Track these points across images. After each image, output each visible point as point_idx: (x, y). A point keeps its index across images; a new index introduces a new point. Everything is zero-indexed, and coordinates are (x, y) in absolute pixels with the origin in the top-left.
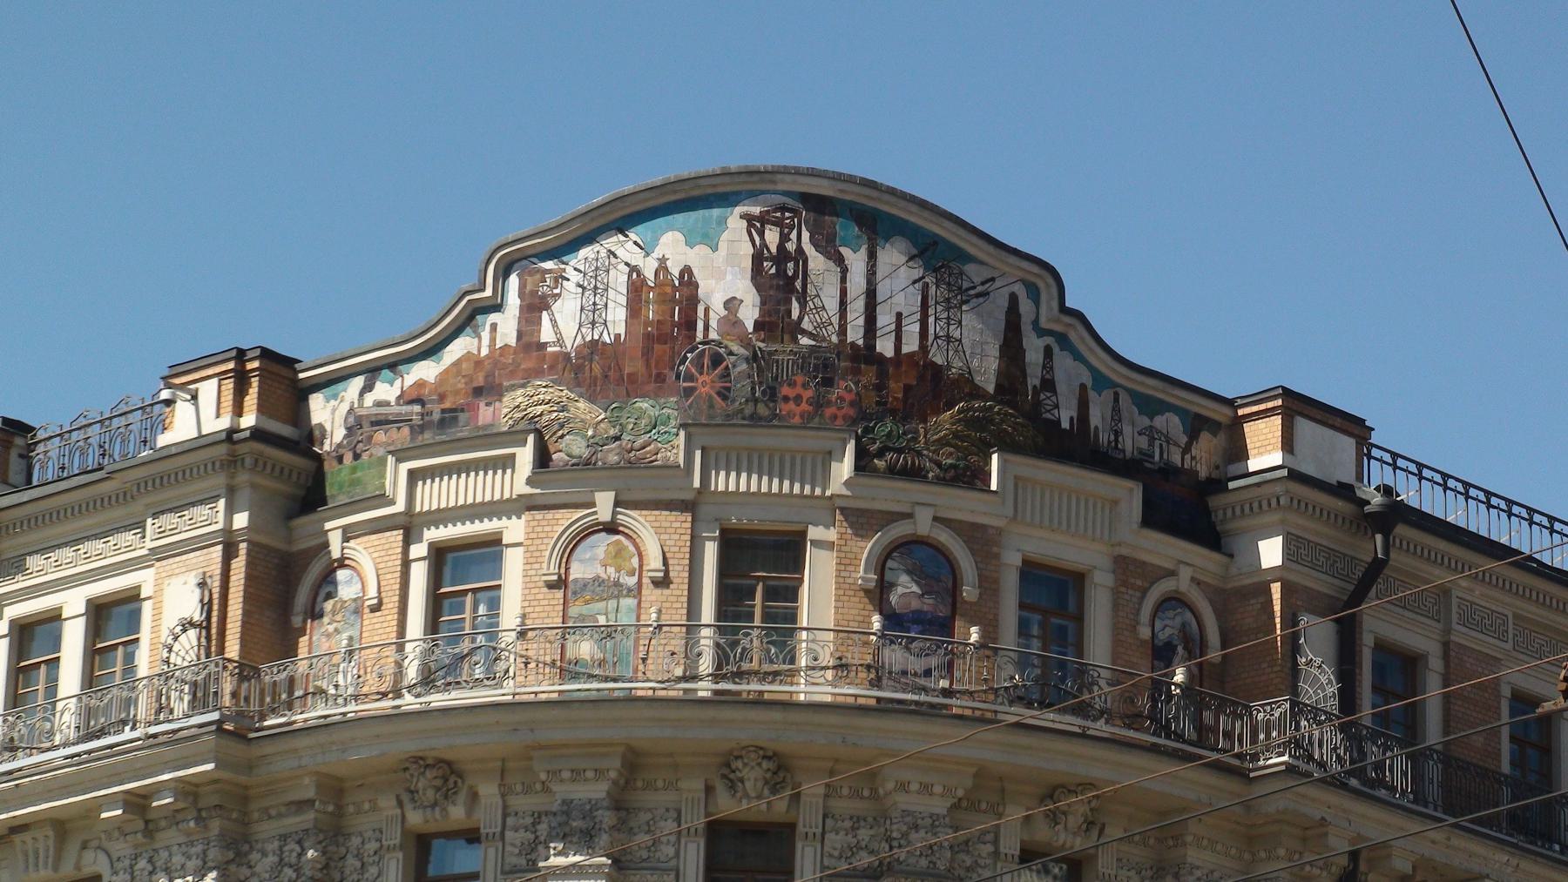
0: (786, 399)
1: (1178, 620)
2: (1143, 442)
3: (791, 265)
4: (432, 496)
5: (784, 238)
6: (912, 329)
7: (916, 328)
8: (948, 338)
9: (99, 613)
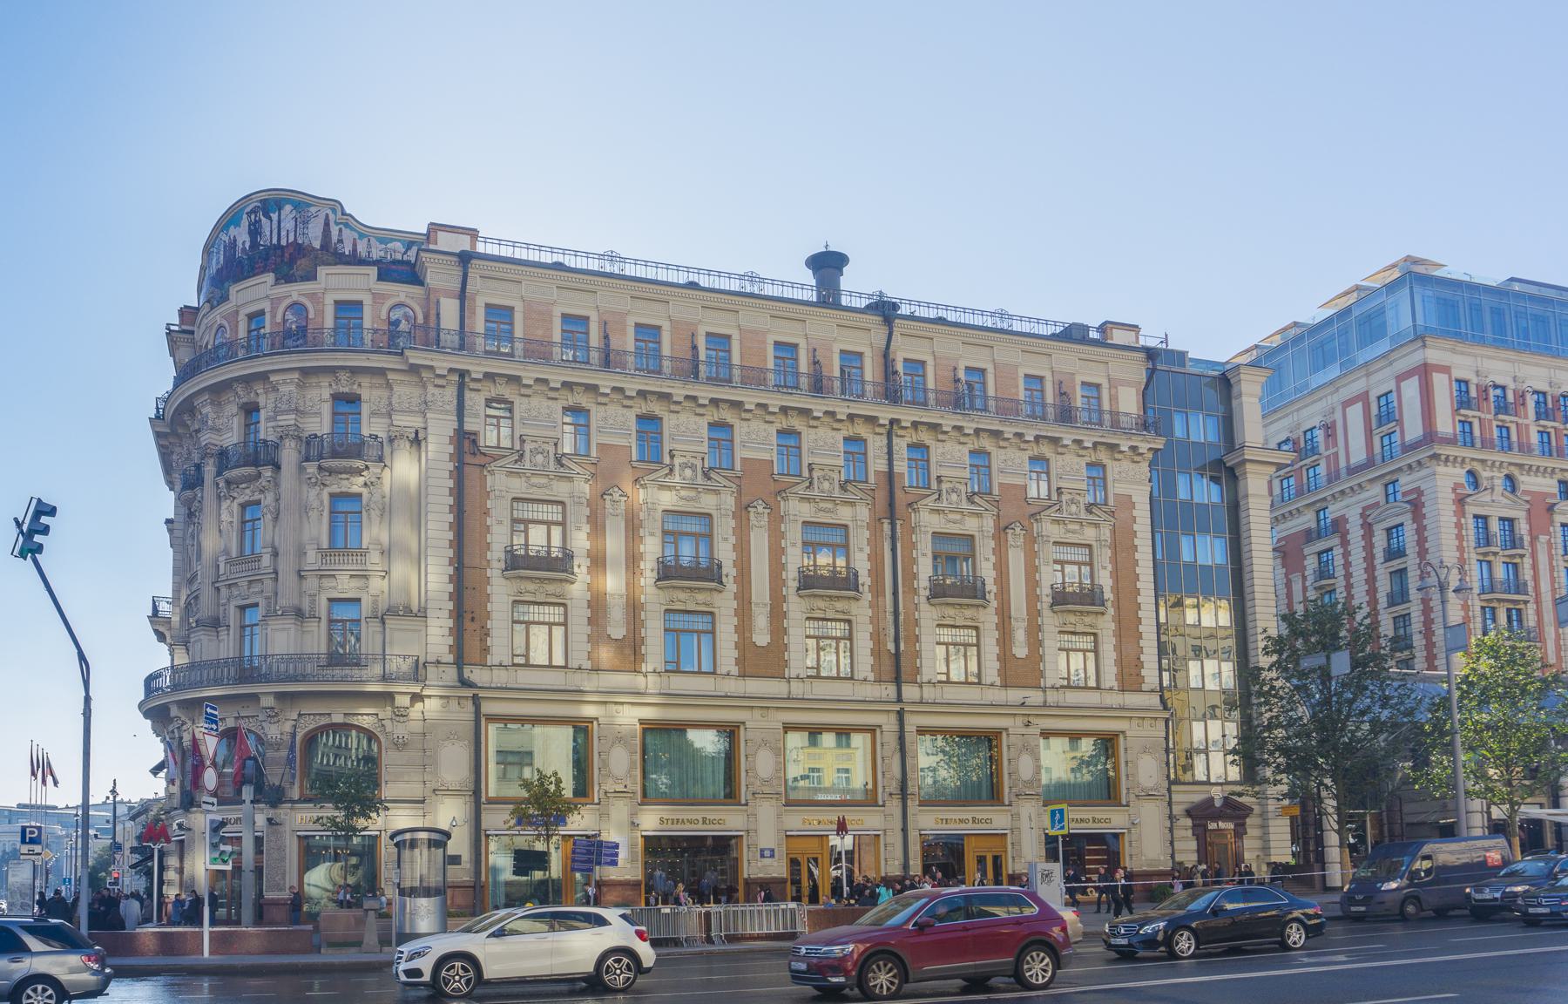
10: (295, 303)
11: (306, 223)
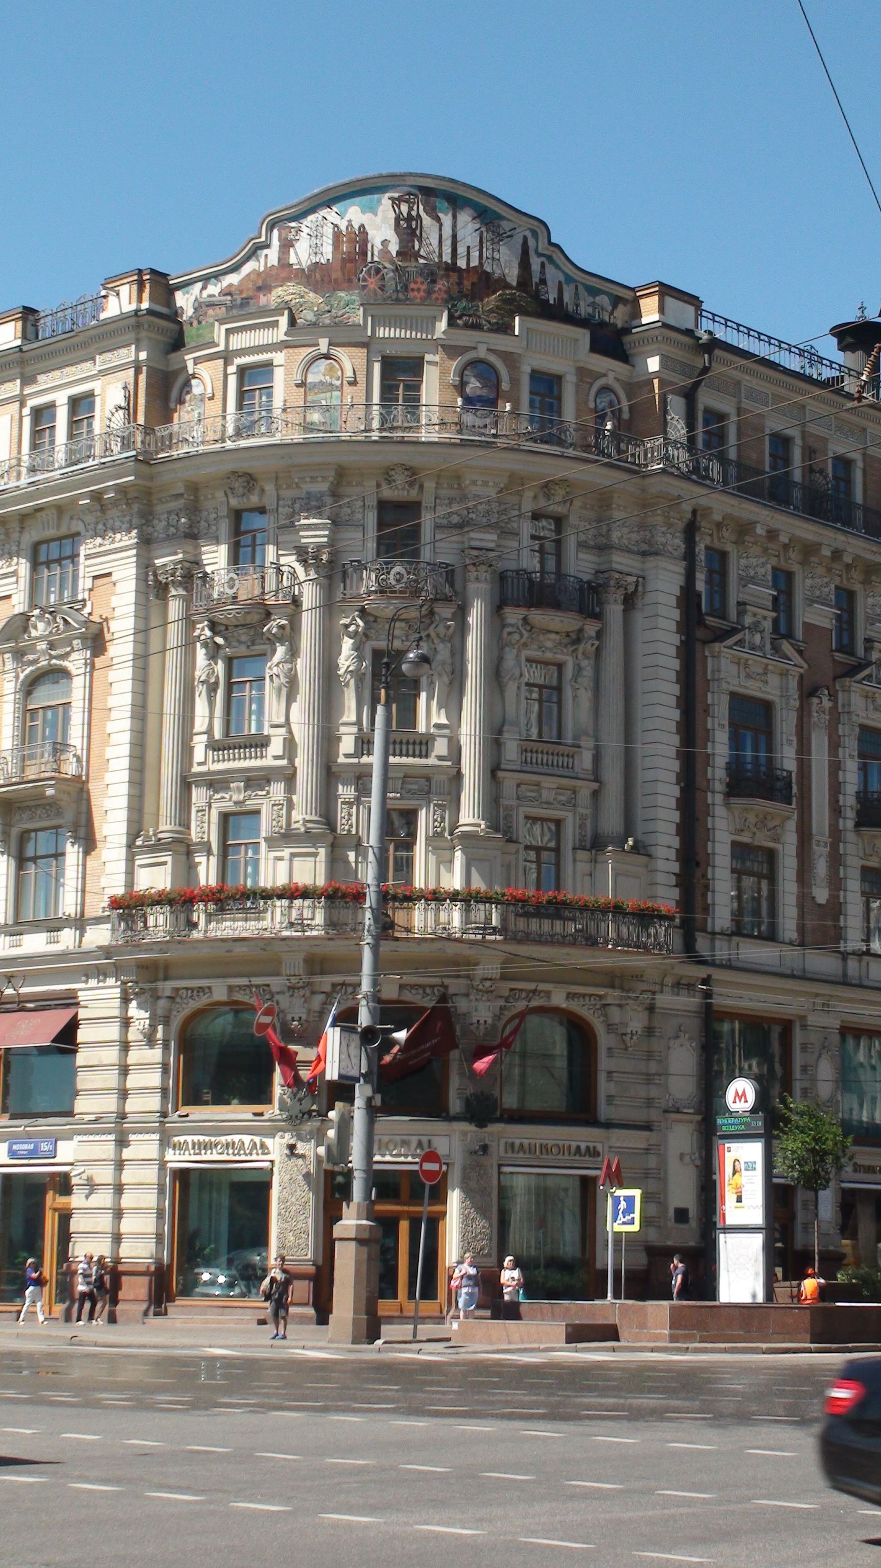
0: (413, 290)
1: (608, 399)
2: (590, 310)
3: (414, 223)
4: (238, 341)
5: (410, 209)
6: (475, 254)
7: (477, 253)
8: (493, 258)
9: (75, 403)
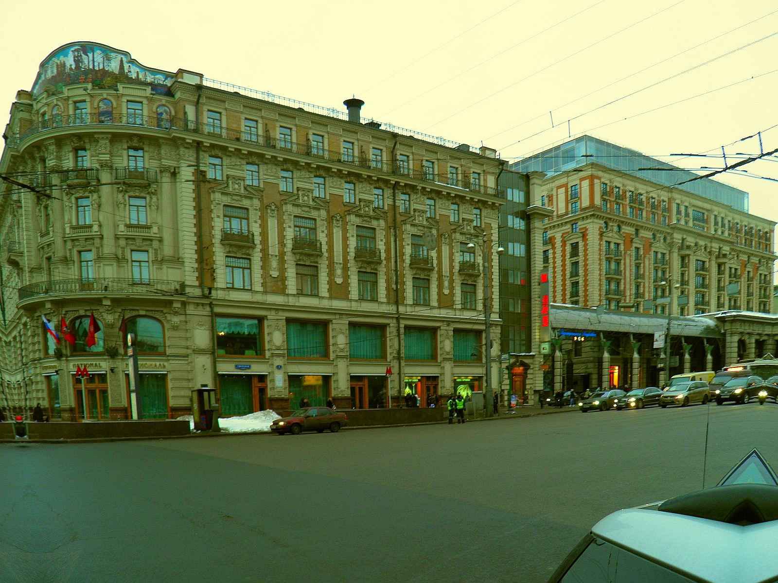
2: (153, 80)
10: (105, 99)
11: (109, 59)
